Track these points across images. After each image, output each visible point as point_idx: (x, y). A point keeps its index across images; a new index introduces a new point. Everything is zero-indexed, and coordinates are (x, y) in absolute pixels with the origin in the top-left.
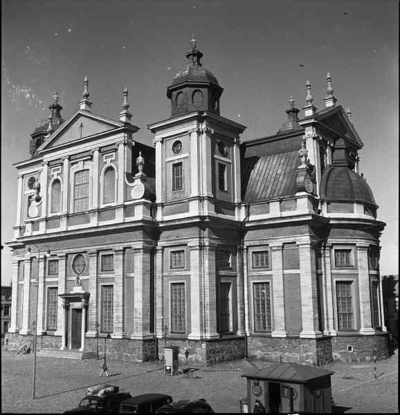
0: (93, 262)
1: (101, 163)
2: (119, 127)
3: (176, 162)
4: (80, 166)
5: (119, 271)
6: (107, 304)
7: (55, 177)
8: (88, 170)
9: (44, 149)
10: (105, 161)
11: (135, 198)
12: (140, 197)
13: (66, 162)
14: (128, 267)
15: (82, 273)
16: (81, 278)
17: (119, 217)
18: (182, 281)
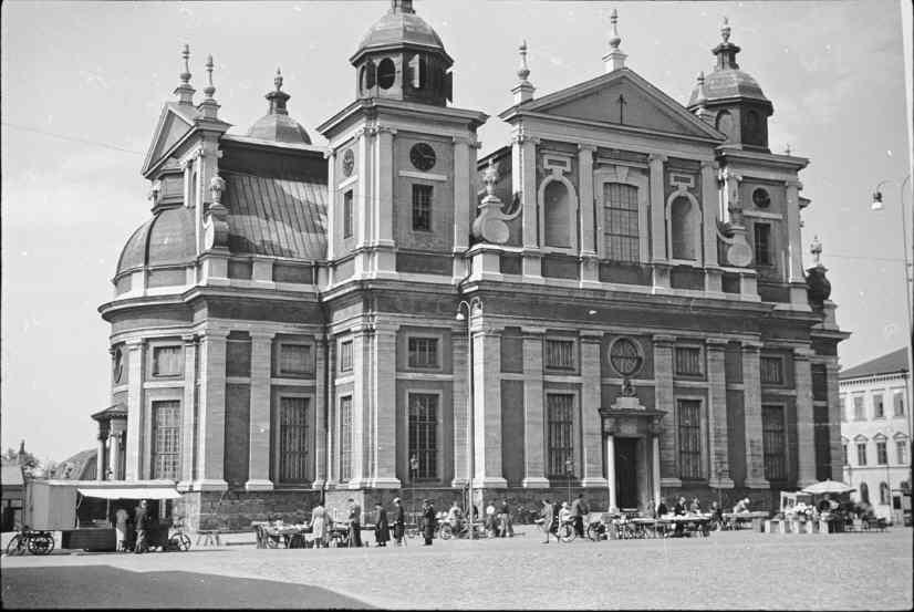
0: (663, 359)
1: (669, 188)
2: (712, 138)
3: (761, 221)
4: (622, 175)
5: (717, 380)
6: (689, 430)
7: (557, 173)
8: (636, 188)
9: (532, 111)
10: (673, 183)
11: (731, 263)
12: (745, 264)
13: (586, 159)
14: (733, 375)
15: (635, 374)
16: (634, 382)
17: (712, 291)
18: (780, 404)
